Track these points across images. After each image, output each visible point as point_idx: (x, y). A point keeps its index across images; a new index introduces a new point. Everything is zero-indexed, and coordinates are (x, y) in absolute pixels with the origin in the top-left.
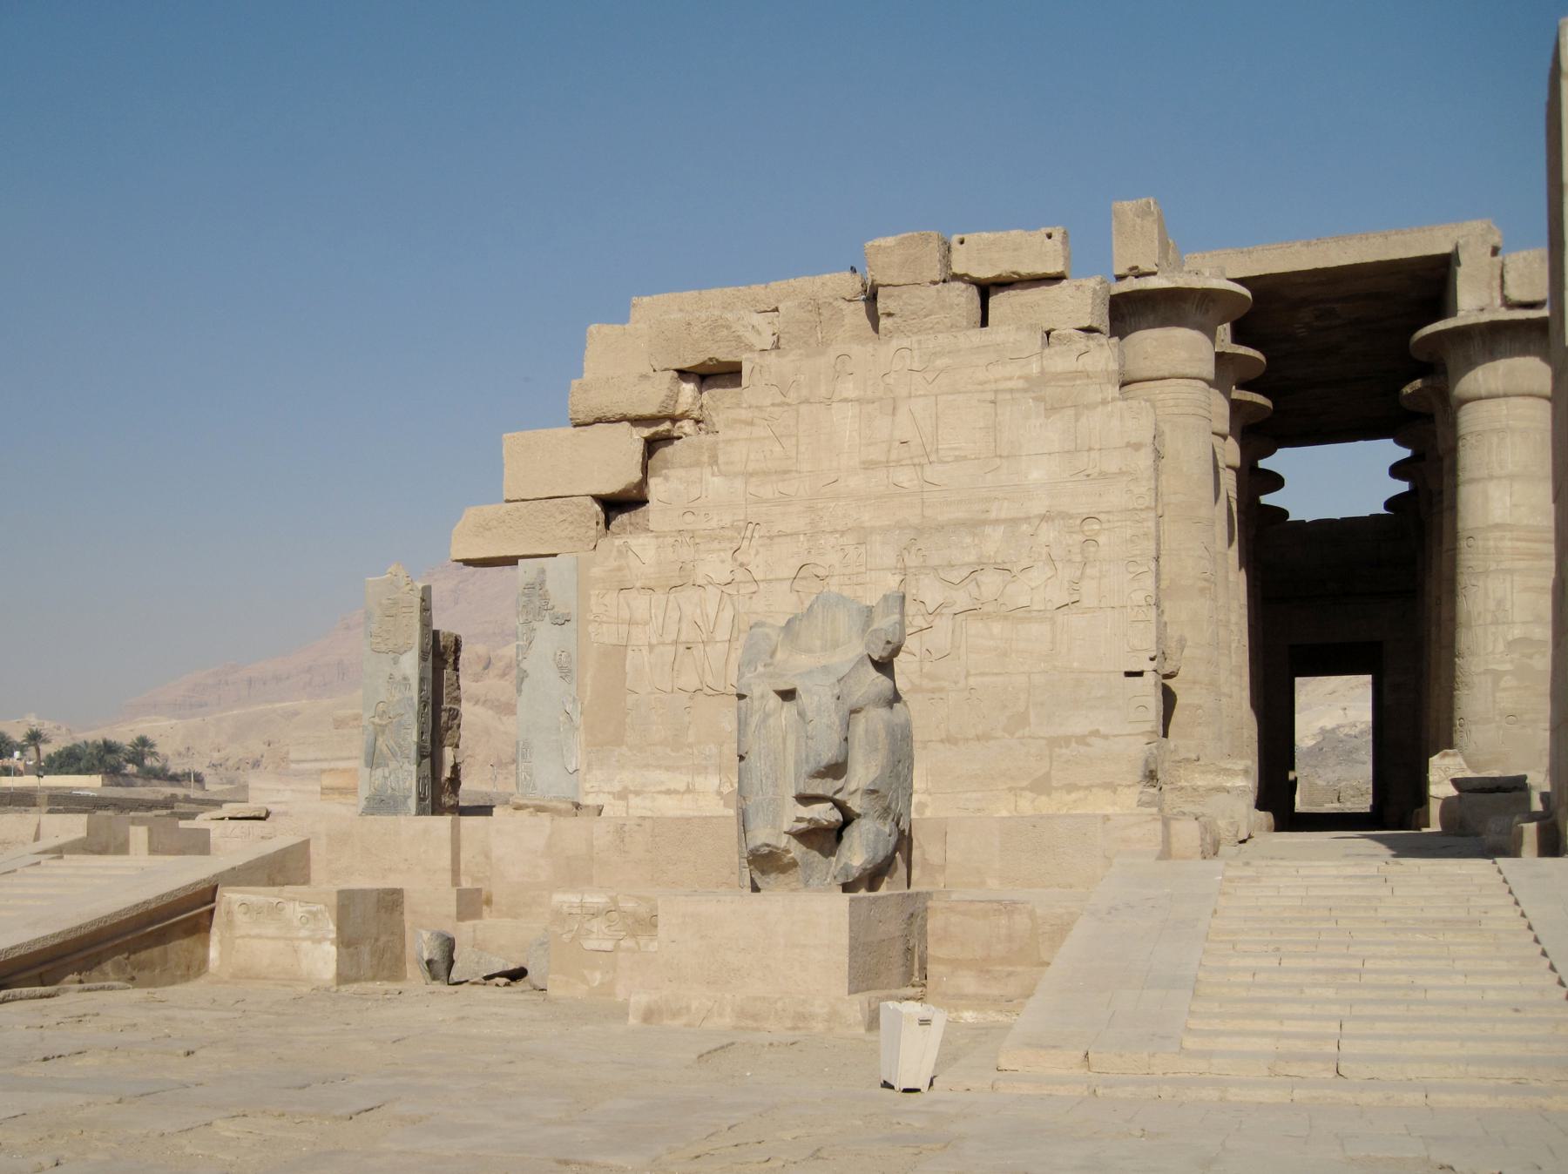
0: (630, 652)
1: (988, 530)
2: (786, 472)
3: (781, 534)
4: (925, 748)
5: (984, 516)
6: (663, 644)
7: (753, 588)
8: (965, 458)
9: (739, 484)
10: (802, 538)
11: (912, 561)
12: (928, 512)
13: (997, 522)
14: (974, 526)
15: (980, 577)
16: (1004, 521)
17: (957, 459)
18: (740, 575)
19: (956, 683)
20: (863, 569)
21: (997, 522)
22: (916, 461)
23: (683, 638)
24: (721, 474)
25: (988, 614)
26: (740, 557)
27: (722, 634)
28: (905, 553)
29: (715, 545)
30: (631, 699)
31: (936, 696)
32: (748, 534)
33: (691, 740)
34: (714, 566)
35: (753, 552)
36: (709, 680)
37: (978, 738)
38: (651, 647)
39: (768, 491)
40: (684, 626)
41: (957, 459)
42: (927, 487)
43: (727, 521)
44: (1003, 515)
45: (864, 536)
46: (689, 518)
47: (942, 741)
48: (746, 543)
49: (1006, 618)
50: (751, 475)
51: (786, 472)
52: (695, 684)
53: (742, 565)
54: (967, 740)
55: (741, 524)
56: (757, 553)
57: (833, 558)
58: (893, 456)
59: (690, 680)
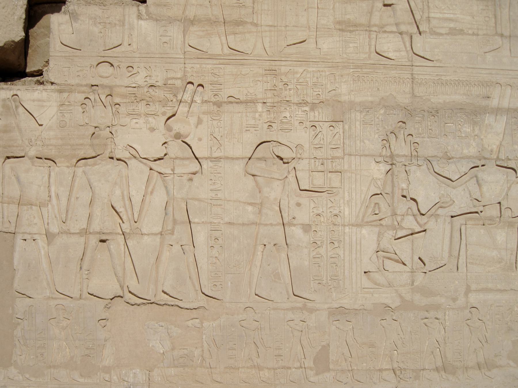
0: (19, 242)
1: (489, 119)
2: (239, 23)
3: (233, 101)
4: (417, 378)
5: (484, 103)
6: (68, 233)
7: (194, 166)
8: (461, 32)
9: (175, 32)
10: (260, 107)
11: (401, 148)
12: (420, 91)
13: (497, 111)
14: (474, 113)
15: (482, 174)
16: (508, 110)
17: (453, 32)
18: (175, 149)
19: (454, 300)
20: (339, 153)
21: (497, 111)
22: (403, 28)
23: (96, 226)
24: (150, 17)
25: (491, 219)
26: (176, 125)
27: (151, 223)
28: (392, 137)
29: (142, 108)
30: (21, 304)
31: (432, 314)
32: (187, 97)
33: (108, 361)
34: (141, 134)
35: (193, 120)
36: (132, 284)
37: (479, 366)
38: (50, 237)
39: (216, 45)
40: (97, 212)
41: (453, 32)
42: (418, 61)
43: (158, 76)
44: (505, 104)
45: (340, 112)
46: (105, 69)
47: (437, 369)
48: (183, 109)
49: (511, 225)
50: (192, 22)
51: (239, 23)
52: (113, 288)
53: (178, 136)
54: (467, 368)
55: (178, 83)
56: (200, 122)
57: (301, 136)
58: (376, 20)
59: (105, 284)
